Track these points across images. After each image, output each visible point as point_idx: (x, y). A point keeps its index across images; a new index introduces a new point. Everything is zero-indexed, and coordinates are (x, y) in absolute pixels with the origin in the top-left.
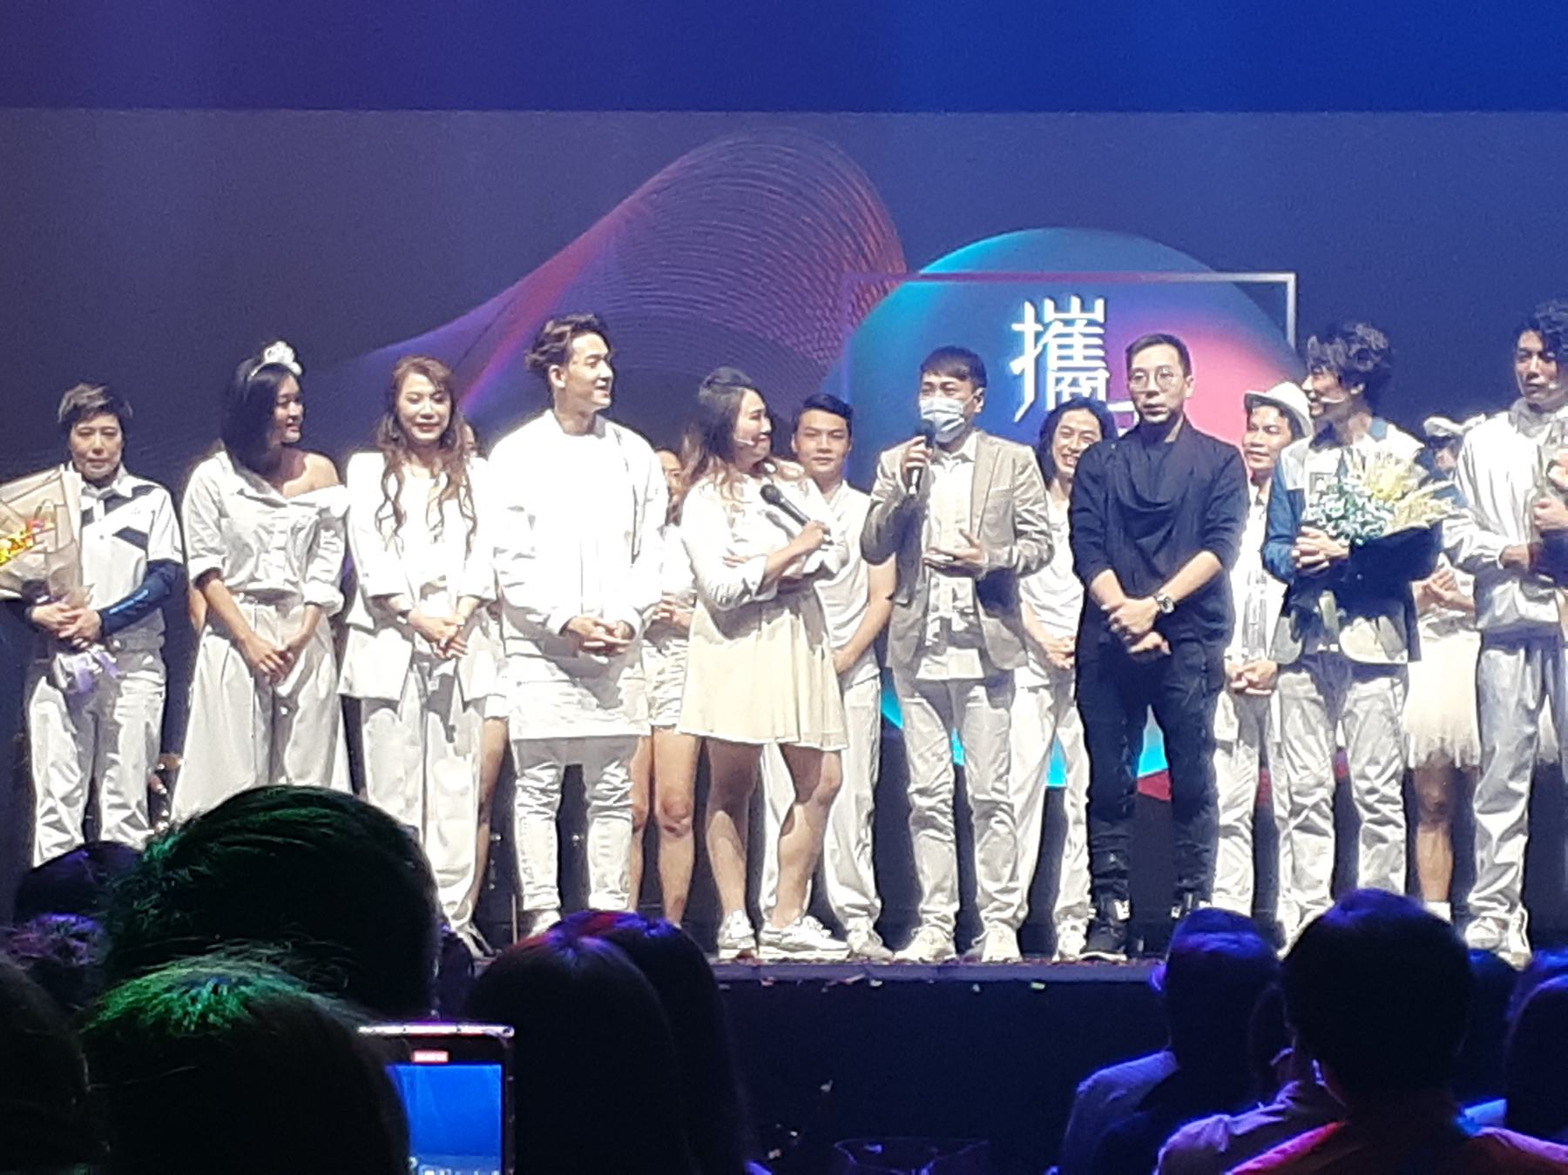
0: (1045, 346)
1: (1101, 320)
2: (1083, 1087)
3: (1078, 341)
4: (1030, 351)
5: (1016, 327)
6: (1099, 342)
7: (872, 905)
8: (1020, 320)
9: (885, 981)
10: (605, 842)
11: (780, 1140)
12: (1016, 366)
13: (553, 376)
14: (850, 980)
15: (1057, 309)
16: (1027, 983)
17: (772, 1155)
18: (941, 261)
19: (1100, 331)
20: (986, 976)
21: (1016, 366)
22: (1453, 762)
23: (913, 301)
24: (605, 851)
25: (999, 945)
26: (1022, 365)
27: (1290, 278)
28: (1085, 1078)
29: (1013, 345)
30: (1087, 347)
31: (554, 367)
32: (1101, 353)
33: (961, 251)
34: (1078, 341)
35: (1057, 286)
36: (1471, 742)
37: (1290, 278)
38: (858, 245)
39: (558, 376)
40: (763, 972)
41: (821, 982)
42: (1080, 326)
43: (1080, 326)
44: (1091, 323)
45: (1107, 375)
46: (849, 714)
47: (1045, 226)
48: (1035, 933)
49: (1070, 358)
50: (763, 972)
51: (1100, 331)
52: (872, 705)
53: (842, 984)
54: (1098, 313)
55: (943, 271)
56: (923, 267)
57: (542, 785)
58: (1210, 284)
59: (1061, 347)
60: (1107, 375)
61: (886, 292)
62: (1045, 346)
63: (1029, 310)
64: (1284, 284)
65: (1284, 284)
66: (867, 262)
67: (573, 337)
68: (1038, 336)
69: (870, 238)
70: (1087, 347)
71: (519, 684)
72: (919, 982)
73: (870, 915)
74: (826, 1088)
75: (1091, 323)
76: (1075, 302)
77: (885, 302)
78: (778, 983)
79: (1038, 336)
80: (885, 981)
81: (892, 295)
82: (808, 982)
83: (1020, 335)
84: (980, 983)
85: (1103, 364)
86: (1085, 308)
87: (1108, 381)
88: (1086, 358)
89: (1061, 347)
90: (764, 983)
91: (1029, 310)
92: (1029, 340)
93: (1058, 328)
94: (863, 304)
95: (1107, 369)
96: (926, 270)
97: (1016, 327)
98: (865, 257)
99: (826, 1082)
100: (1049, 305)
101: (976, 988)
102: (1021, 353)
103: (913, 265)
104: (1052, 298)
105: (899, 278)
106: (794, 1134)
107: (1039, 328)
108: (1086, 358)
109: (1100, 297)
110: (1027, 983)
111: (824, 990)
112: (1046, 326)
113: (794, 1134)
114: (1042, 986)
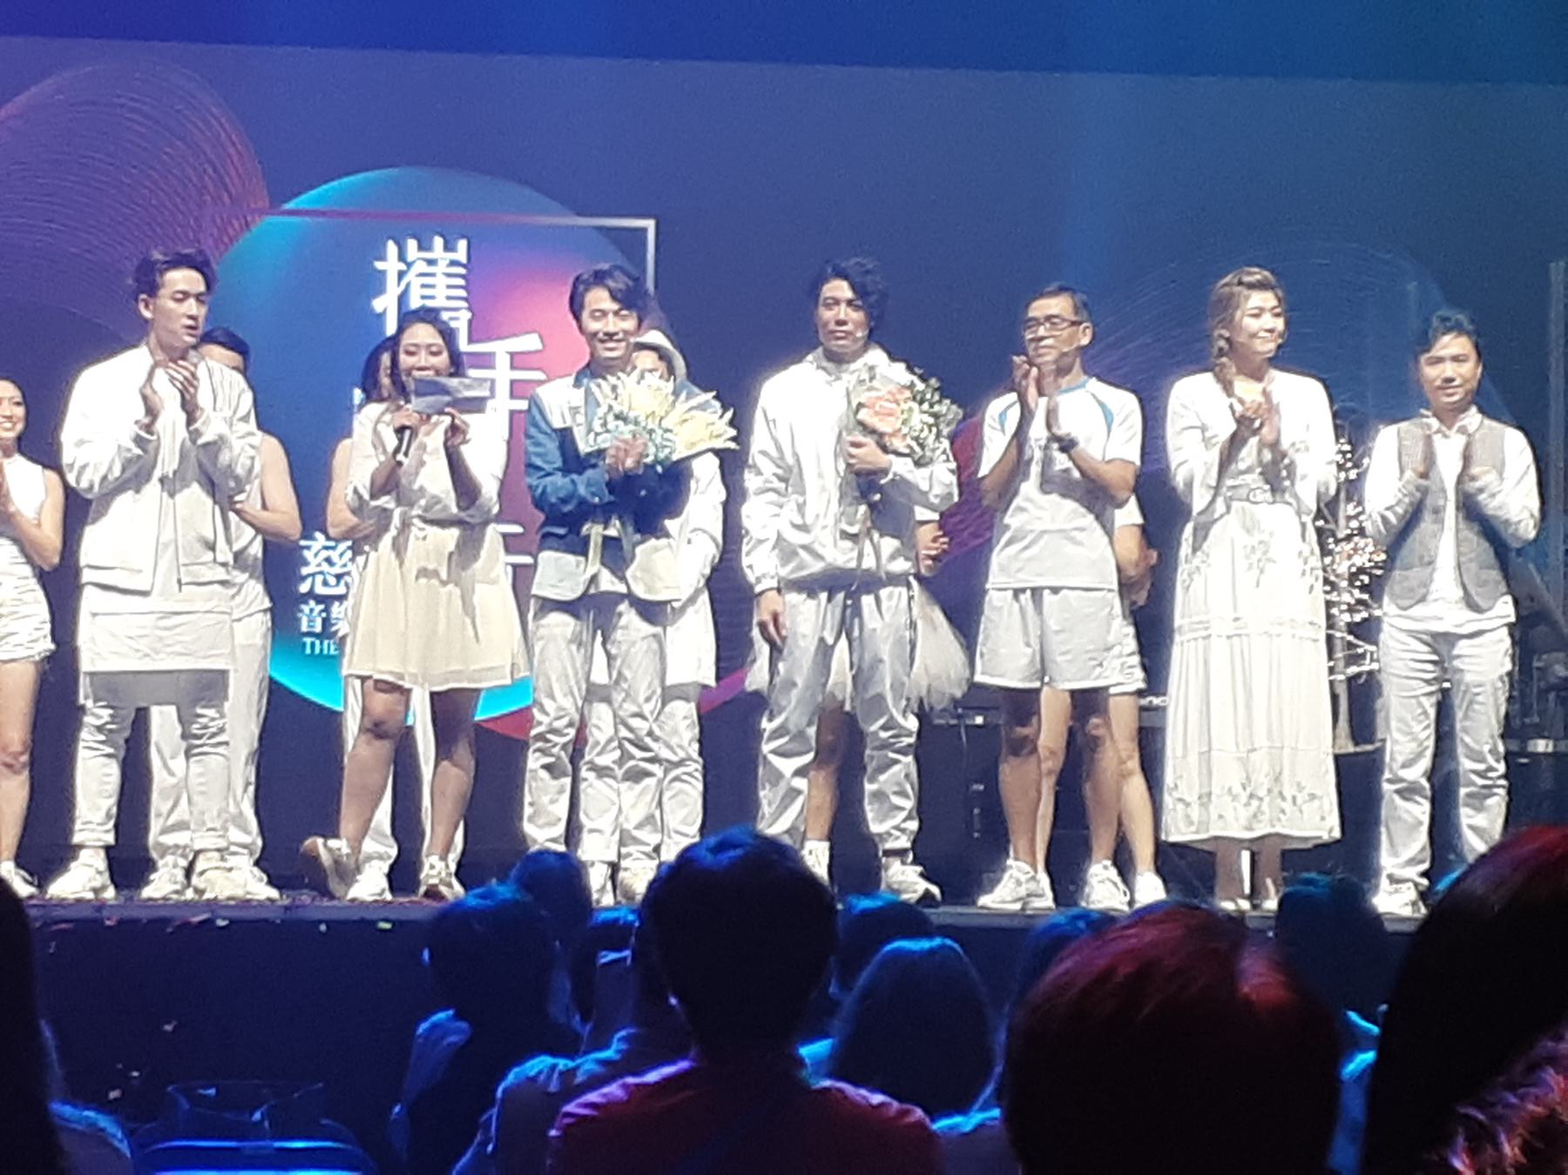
0: (408, 285)
1: (464, 260)
2: (423, 1027)
3: (441, 281)
4: (393, 290)
5: (379, 265)
6: (461, 282)
7: (254, 843)
8: (383, 258)
9: (232, 922)
10: (202, 780)
11: (122, 1081)
12: (378, 304)
13: (142, 307)
14: (196, 919)
15: (421, 248)
16: (374, 922)
17: (113, 1095)
18: (304, 197)
19: (462, 271)
20: (343, 916)
21: (378, 304)
22: (843, 703)
23: (274, 237)
24: (203, 788)
25: (370, 885)
26: (385, 304)
27: (650, 224)
28: (425, 1019)
29: (376, 284)
30: (449, 287)
31: (143, 296)
32: (463, 293)
33: (325, 187)
34: (441, 281)
35: (420, 225)
36: (844, 684)
37: (650, 224)
38: (221, 177)
39: (147, 306)
40: (105, 913)
41: (165, 921)
42: (442, 267)
43: (442, 267)
44: (453, 263)
45: (468, 315)
46: (238, 651)
47: (410, 163)
48: (403, 874)
49: (432, 297)
50: (105, 913)
51: (462, 271)
52: (259, 641)
53: (187, 924)
54: (461, 254)
55: (306, 207)
56: (289, 199)
57: (99, 723)
58: (559, 227)
59: (423, 286)
60: (468, 315)
61: (247, 225)
62: (408, 285)
63: (392, 248)
64: (644, 230)
65: (644, 230)
66: (230, 196)
67: (167, 270)
68: (401, 275)
69: (233, 173)
70: (449, 287)
71: (95, 615)
72: (266, 921)
73: (251, 854)
74: (168, 1028)
75: (453, 263)
76: (438, 242)
77: (247, 235)
78: (121, 922)
79: (401, 275)
80: (232, 922)
81: (254, 229)
82: (150, 921)
83: (383, 273)
84: (327, 922)
85: (464, 304)
86: (449, 247)
87: (470, 322)
88: (449, 298)
89: (423, 286)
90: (108, 923)
91: (392, 248)
92: (392, 278)
93: (421, 267)
94: (226, 239)
95: (470, 309)
96: (290, 206)
97: (379, 265)
98: (227, 190)
99: (169, 1023)
100: (412, 244)
101: (323, 928)
102: (380, 290)
103: (277, 199)
104: (414, 237)
105: (262, 212)
106: (135, 1074)
107: (403, 267)
108: (449, 298)
109: (463, 237)
110: (374, 922)
111: (169, 930)
112: (409, 265)
113: (135, 1074)
114: (387, 926)
